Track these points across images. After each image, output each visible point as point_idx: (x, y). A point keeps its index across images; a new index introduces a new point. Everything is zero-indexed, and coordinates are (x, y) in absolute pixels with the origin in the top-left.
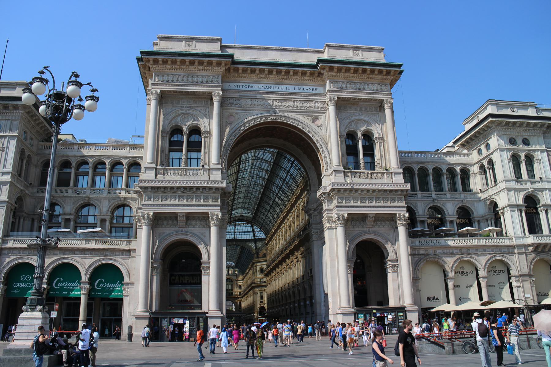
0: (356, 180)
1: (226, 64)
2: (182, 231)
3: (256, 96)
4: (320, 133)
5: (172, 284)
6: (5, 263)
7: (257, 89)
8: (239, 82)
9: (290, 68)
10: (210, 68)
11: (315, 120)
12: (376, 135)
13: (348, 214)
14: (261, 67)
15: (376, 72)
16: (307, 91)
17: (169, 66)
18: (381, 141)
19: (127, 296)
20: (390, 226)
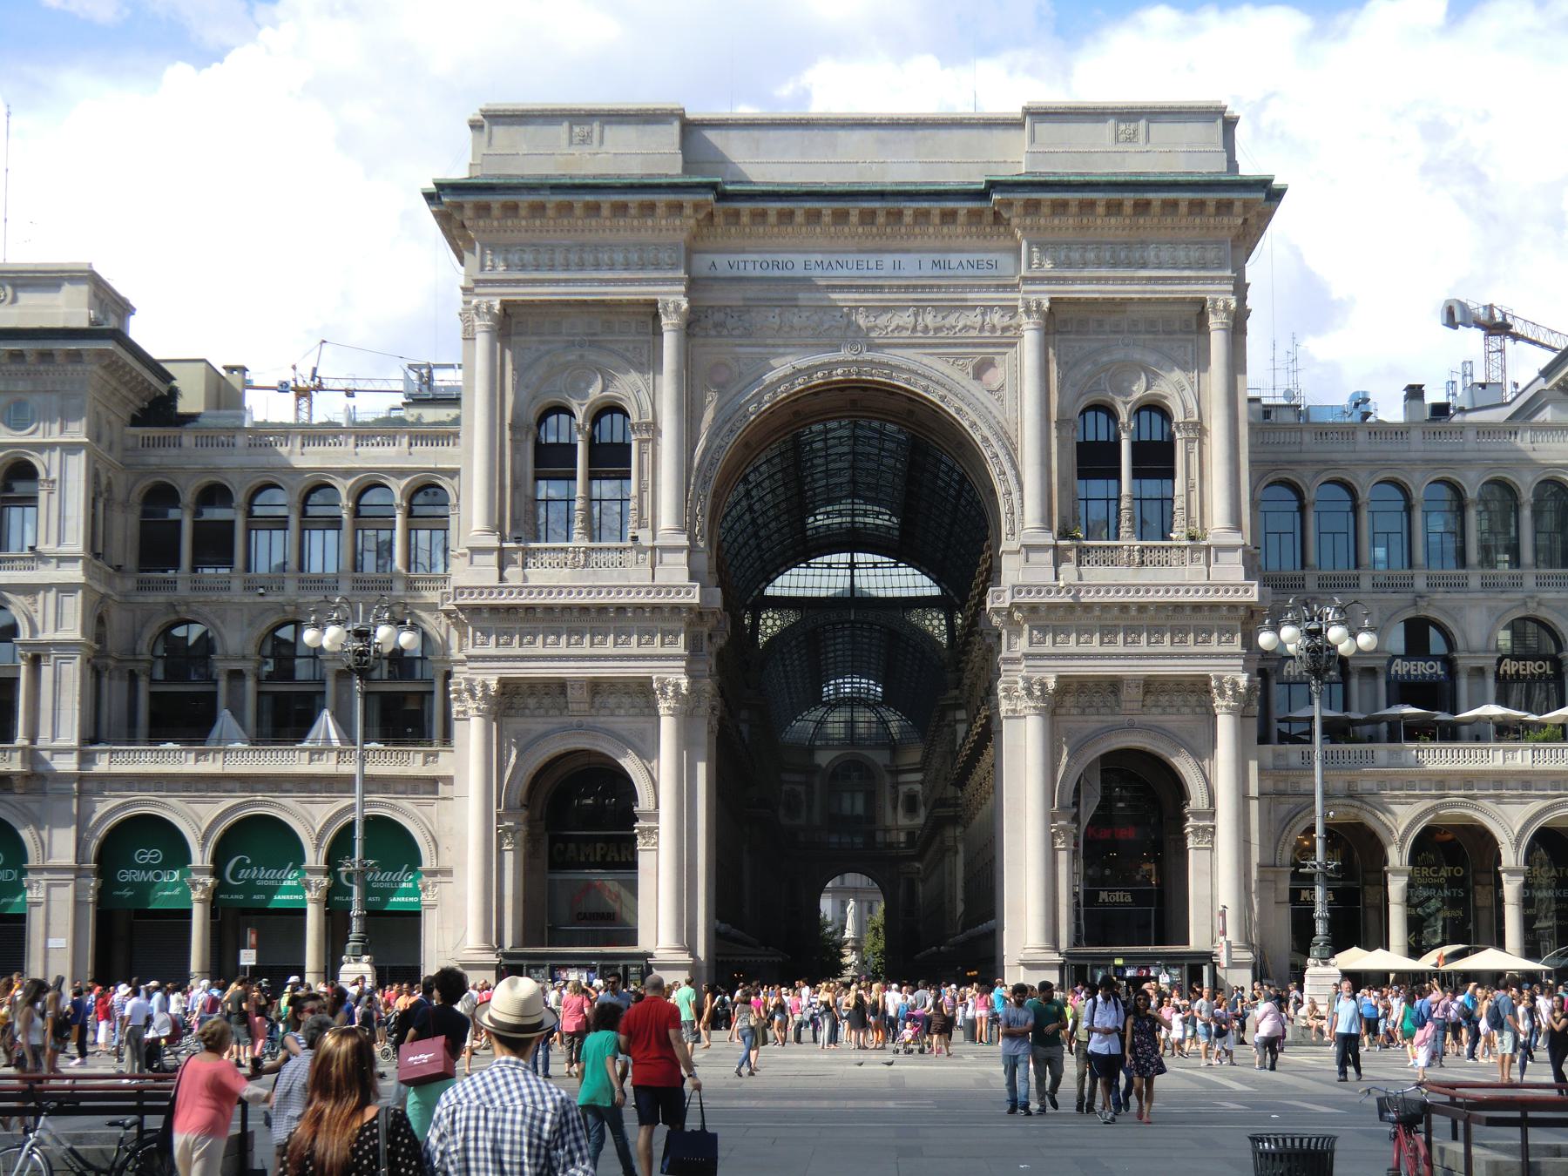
0: (1097, 574)
1: (697, 207)
2: (580, 726)
3: (796, 299)
4: (995, 412)
5: (557, 864)
6: (95, 817)
7: (799, 272)
8: (743, 252)
9: (902, 205)
10: (650, 222)
11: (979, 371)
12: (1178, 416)
13: (1060, 678)
14: (808, 205)
15: (1183, 209)
16: (960, 272)
17: (524, 223)
18: (1191, 435)
19: (433, 907)
20: (1198, 709)
